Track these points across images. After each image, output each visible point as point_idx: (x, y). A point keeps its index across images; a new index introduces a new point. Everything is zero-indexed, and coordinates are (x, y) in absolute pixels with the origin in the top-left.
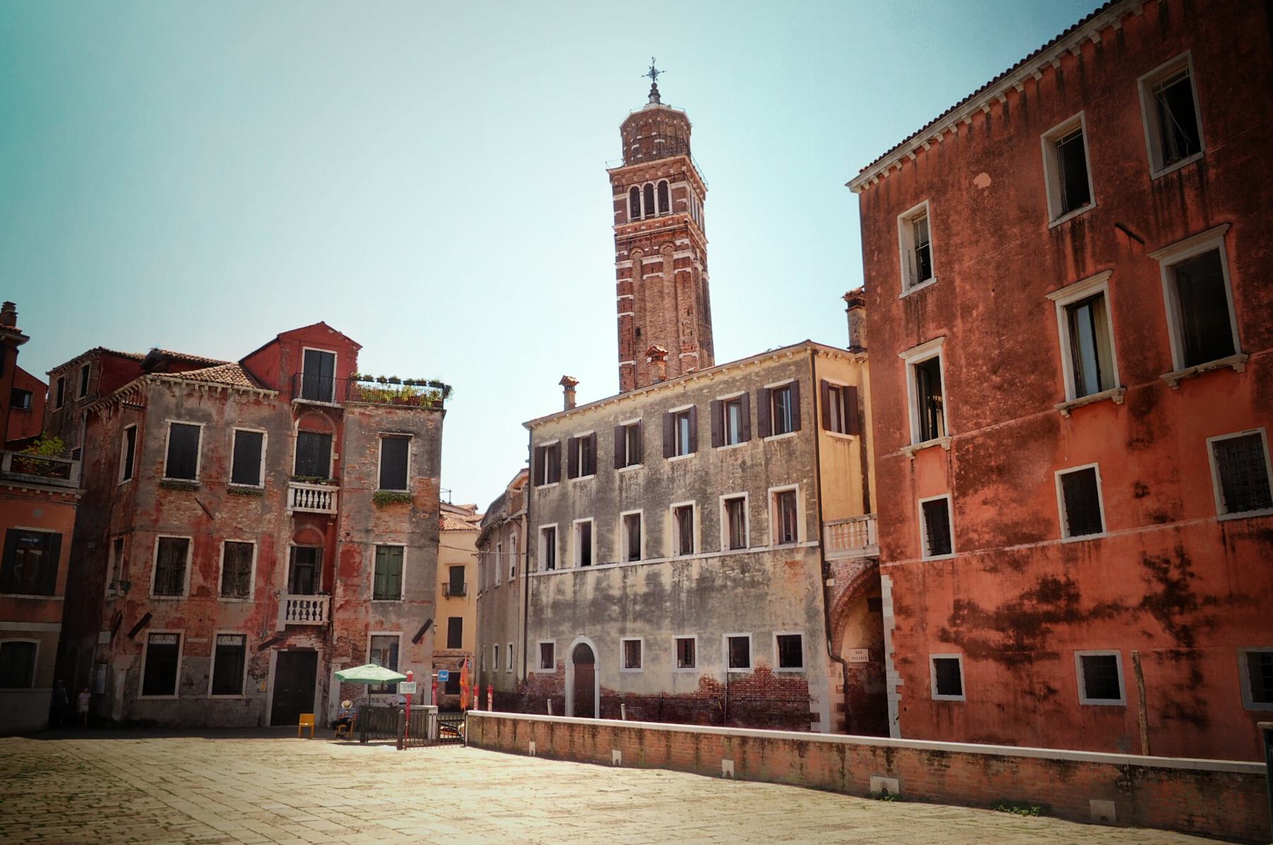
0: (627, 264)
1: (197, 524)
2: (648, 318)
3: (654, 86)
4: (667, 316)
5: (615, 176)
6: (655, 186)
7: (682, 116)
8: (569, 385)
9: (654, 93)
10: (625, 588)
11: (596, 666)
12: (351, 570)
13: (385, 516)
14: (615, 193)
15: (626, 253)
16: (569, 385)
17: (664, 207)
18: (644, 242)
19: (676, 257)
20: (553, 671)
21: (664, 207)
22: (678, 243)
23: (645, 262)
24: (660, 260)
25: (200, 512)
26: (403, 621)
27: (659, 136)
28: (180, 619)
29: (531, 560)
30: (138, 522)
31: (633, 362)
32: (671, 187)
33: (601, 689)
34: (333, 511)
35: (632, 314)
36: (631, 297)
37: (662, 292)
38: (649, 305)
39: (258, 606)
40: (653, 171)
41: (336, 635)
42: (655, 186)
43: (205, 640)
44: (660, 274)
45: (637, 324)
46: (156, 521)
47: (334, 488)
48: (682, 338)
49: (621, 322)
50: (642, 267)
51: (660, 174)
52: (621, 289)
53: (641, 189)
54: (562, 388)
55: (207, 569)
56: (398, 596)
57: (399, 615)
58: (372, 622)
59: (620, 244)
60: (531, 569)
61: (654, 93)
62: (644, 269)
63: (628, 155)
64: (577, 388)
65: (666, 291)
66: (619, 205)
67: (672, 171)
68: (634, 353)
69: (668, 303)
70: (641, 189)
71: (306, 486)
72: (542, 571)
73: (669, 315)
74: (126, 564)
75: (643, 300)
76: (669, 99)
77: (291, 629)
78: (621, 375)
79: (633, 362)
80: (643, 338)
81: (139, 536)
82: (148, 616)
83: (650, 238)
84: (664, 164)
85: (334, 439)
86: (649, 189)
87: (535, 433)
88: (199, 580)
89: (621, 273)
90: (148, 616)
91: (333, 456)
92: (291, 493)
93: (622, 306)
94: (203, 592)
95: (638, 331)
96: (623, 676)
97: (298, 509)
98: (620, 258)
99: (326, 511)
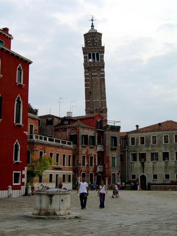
0: (88, 74)
1: (86, 153)
2: (93, 90)
3: (92, 24)
4: (98, 89)
5: (83, 49)
6: (96, 54)
7: (100, 35)
8: (137, 126)
9: (92, 26)
10: (153, 165)
11: (147, 179)
12: (108, 161)
13: (113, 152)
14: (84, 54)
15: (87, 71)
16: (137, 126)
17: (98, 60)
18: (92, 69)
19: (101, 74)
20: (136, 179)
21: (98, 60)
22: (102, 70)
23: (92, 74)
24: (97, 74)
25: (87, 151)
26: (116, 171)
27: (96, 40)
28: (85, 170)
29: (129, 159)
30: (80, 153)
31: (89, 101)
32: (100, 55)
33: (148, 183)
34: (103, 150)
35: (89, 88)
36: (89, 83)
37: (97, 83)
38: (94, 86)
39: (94, 168)
40: (95, 50)
41: (106, 173)
42: (96, 54)
43: (88, 174)
44: (97, 78)
45: (90, 90)
46: (82, 153)
47: (103, 146)
48: (102, 96)
49: (86, 90)
50: (92, 75)
51: (97, 50)
52: (86, 81)
53: (92, 54)
54: (136, 127)
55: (88, 162)
56: (115, 166)
57: (115, 170)
58: (112, 171)
59: (85, 68)
60: (129, 161)
61: (92, 26)
62: (92, 76)
63: (86, 43)
64: (139, 127)
65: (98, 83)
66: (85, 57)
67: (100, 50)
68: (89, 98)
69: (99, 86)
70: (92, 54)
71: (100, 146)
72: (131, 161)
73: (99, 89)
74: (78, 161)
75: (92, 84)
76: (98, 29)
77: (99, 172)
78: (86, 104)
79: (89, 101)
80: (92, 94)
81: (80, 155)
82: (82, 170)
83: (94, 67)
84: (98, 48)
85: (102, 136)
86: (94, 54)
87: (129, 135)
88: (87, 163)
89: (86, 76)
90: (82, 170)
91: (102, 140)
92: (98, 147)
93: (86, 85)
94: (88, 166)
95: (90, 93)
96: (153, 180)
97: (99, 150)
98: (85, 72)
99: (101, 150)
